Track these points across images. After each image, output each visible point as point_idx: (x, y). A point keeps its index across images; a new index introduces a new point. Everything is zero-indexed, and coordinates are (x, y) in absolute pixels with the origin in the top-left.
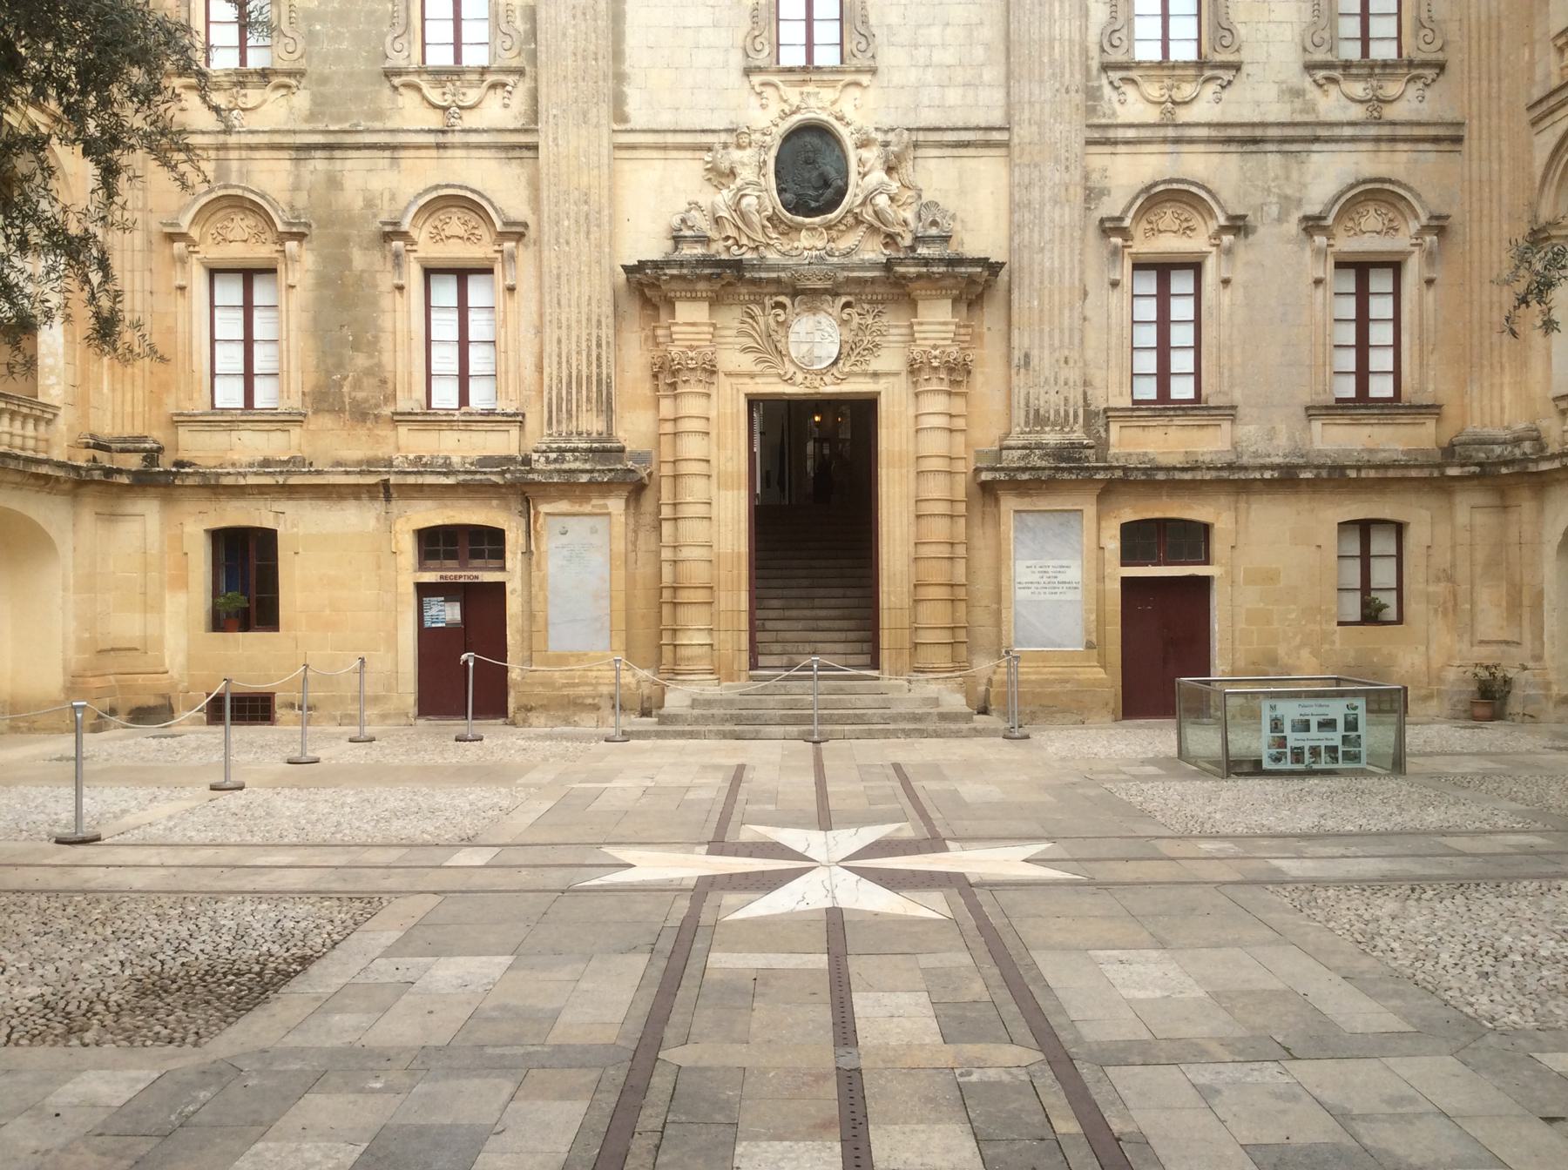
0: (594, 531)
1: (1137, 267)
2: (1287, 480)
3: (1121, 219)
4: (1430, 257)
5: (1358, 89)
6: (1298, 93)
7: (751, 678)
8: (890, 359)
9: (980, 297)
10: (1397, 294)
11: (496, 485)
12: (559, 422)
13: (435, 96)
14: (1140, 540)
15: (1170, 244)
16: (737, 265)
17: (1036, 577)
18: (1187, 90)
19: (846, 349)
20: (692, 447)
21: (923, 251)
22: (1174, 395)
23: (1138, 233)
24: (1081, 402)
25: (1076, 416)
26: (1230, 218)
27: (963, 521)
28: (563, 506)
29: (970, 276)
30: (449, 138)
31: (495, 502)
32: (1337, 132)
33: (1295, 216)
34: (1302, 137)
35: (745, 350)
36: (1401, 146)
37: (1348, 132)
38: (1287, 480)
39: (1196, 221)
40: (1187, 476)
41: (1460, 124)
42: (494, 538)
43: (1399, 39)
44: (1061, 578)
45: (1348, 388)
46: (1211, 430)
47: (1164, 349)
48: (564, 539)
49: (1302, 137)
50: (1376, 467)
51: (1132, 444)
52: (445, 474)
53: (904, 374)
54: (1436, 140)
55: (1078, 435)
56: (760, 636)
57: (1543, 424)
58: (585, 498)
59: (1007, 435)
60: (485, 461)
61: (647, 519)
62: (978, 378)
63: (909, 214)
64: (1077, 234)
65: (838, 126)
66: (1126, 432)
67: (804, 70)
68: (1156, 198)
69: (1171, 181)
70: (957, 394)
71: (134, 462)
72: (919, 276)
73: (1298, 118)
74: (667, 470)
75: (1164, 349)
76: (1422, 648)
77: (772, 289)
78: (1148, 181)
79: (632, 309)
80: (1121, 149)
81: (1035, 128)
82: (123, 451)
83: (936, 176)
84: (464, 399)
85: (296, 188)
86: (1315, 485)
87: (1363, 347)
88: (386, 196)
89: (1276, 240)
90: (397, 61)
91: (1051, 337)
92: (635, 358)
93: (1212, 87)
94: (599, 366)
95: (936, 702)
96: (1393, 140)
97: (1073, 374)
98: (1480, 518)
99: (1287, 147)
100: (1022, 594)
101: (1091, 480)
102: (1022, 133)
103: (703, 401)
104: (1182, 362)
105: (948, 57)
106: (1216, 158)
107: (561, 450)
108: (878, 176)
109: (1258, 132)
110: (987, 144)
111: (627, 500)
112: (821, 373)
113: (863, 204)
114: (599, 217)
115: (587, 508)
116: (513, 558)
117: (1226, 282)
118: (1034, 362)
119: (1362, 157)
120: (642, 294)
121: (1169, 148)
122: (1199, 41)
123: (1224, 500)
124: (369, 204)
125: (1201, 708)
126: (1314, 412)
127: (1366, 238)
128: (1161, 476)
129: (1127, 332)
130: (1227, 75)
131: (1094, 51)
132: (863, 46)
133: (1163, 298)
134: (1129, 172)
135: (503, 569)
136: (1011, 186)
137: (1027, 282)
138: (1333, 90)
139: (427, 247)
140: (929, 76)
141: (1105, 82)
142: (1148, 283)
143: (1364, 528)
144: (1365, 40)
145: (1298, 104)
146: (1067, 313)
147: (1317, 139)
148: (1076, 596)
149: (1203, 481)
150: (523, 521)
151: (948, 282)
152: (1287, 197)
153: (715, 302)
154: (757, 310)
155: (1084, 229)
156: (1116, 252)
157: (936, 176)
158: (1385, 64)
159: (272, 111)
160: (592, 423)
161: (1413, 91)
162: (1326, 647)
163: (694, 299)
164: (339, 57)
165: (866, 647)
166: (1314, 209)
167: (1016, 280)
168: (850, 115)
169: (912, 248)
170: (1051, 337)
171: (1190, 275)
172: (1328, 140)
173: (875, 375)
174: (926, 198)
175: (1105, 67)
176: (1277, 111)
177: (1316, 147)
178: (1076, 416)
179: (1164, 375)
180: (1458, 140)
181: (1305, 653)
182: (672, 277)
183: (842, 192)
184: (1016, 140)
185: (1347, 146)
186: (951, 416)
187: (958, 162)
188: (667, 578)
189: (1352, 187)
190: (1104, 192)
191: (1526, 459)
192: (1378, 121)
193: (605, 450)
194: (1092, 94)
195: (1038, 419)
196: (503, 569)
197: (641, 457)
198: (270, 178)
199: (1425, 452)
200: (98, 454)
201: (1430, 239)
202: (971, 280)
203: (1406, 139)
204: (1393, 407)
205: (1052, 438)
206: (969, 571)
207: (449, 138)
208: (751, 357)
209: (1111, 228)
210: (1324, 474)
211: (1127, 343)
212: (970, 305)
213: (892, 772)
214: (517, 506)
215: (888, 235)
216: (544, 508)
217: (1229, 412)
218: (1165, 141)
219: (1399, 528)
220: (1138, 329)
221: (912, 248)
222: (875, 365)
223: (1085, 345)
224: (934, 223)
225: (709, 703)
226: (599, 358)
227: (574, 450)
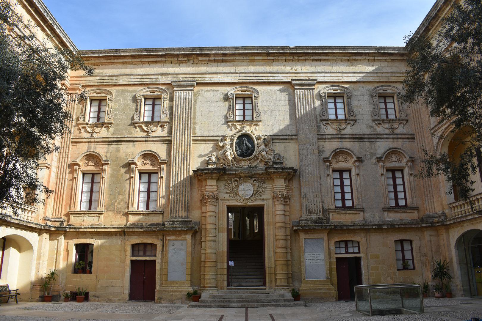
0: (182, 245)
1: (334, 171)
2: (380, 228)
3: (328, 158)
4: (411, 168)
5: (387, 126)
6: (372, 127)
7: (227, 289)
8: (267, 195)
9: (292, 178)
10: (403, 178)
11: (155, 231)
12: (173, 213)
13: (145, 128)
15: (342, 165)
16: (224, 169)
17: (311, 258)
18: (343, 126)
19: (255, 192)
20: (210, 220)
21: (275, 166)
22: (347, 205)
23: (333, 162)
24: (321, 207)
25: (320, 211)
26: (357, 158)
27: (289, 241)
28: (173, 237)
29: (289, 172)
30: (148, 139)
31: (154, 236)
32: (383, 136)
33: (374, 158)
34: (374, 137)
35: (226, 193)
36: (399, 140)
37: (386, 136)
38: (380, 228)
39: (348, 159)
40: (352, 228)
41: (414, 135)
42: (153, 246)
44: (319, 258)
45: (393, 203)
46: (358, 215)
47: (343, 193)
48: (173, 247)
49: (374, 137)
50: (403, 225)
51: (336, 218)
52: (141, 228)
53: (271, 200)
54: (408, 138)
55: (321, 216)
56: (230, 277)
57: (446, 211)
58: (180, 235)
59: (301, 216)
60: (152, 225)
61: (198, 241)
62: (292, 201)
63: (271, 157)
64: (317, 162)
65: (252, 134)
66: (334, 215)
67: (243, 121)
68: (337, 153)
69: (341, 148)
70: (286, 205)
71: (57, 224)
72: (275, 172)
73: (372, 133)
74: (203, 227)
75: (343, 193)
76: (421, 276)
77: (234, 176)
78: (335, 149)
79: (195, 182)
80: (327, 140)
81: (304, 135)
82: (54, 221)
83: (278, 147)
84: (148, 208)
85: (107, 152)
86: (387, 230)
87: (396, 192)
88: (131, 153)
89: (370, 164)
90: (136, 120)
91: (312, 189)
92: (196, 195)
93: (349, 125)
94: (185, 198)
95: (283, 296)
96: (397, 138)
97: (319, 199)
98: (432, 238)
99: (370, 140)
100: (307, 263)
101: (325, 229)
102: (301, 136)
103: (214, 207)
105: (281, 118)
106: (352, 143)
107: (173, 221)
108: (263, 147)
109: (362, 137)
110: (292, 139)
111: (192, 236)
112: (248, 199)
113: (259, 154)
114: (186, 158)
115: (180, 238)
116: (159, 254)
117: (358, 175)
118: (308, 196)
119: (390, 143)
120: (198, 178)
121: (340, 140)
122: (345, 114)
123: (362, 234)
124: (126, 156)
125: (362, 297)
127: (393, 163)
128: (345, 228)
129: (332, 188)
130: (353, 123)
131: (318, 117)
132: (258, 115)
133: (342, 179)
134: (330, 146)
135: (155, 256)
136: (299, 150)
137: (304, 174)
138: (381, 126)
139: (140, 166)
140: (276, 123)
141: (321, 124)
142: (337, 175)
143: (402, 242)
144: (387, 114)
145: (372, 130)
146: (316, 183)
147: (378, 138)
149: (357, 229)
150: (162, 242)
151: (283, 174)
152: (372, 153)
153: (218, 180)
154: (230, 182)
155: (319, 161)
156: (328, 167)
157: (278, 147)
158: (393, 120)
159: (102, 133)
160: (183, 214)
161: (401, 127)
162: (395, 277)
163: (212, 179)
164: (122, 119)
165: (262, 280)
166: (380, 156)
167: (301, 174)
168: (254, 131)
169: (273, 166)
170: (312, 189)
172: (380, 138)
173: (263, 200)
174: (276, 152)
175: (322, 120)
177: (378, 140)
178: (320, 211)
180: (414, 138)
181: (389, 279)
182: (206, 173)
183: (253, 151)
184: (299, 138)
185: (385, 140)
186: (285, 211)
187: (284, 144)
188: (203, 258)
189: (388, 150)
191: (443, 221)
192: (393, 134)
193: (186, 221)
194: (318, 127)
195: (310, 212)
196: (155, 256)
197: (195, 223)
198: (101, 150)
199: (416, 220)
200: (48, 222)
201: (410, 163)
202: (289, 174)
203: (400, 138)
204: (406, 208)
205: (314, 217)
206: (292, 256)
207: (148, 139)
208: (228, 195)
209: (326, 160)
210: (389, 226)
211: (333, 191)
212: (289, 181)
213: (269, 317)
214: (160, 237)
215: (266, 162)
216: (168, 238)
217: (362, 210)
218: (338, 138)
219: (411, 242)
220: (335, 187)
221: (273, 166)
222: (264, 197)
223: (321, 192)
224: (278, 159)
225: (214, 297)
226: (185, 196)
227: (177, 221)
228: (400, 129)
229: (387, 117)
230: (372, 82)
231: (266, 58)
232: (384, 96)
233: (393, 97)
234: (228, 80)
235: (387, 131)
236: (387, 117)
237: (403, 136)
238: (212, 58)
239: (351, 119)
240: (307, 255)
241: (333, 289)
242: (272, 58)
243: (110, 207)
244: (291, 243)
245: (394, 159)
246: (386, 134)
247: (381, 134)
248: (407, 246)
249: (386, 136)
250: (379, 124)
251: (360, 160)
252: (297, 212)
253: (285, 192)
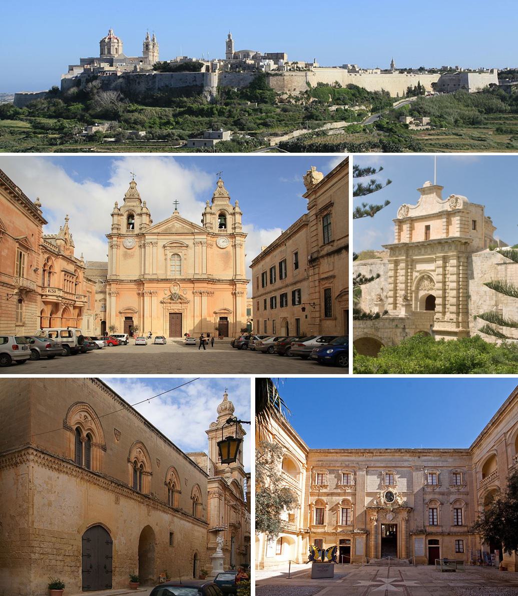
5: (457, 488)
14: (431, 542)
15: (433, 506)
47: (433, 519)
49: (450, 493)
51: (430, 529)
68: (431, 501)
75: (433, 519)
87: (457, 519)
126: (452, 526)
127: (457, 506)
142: (431, 510)
143: (459, 541)
159: (324, 490)
176: (446, 491)
179: (433, 522)
198: (325, 499)
205: (419, 529)
228: (462, 490)
234: (382, 465)
239: (440, 484)
241: (427, 560)
243: (330, 524)
245: (458, 504)
248: (461, 543)
251: (442, 504)
252: (413, 527)
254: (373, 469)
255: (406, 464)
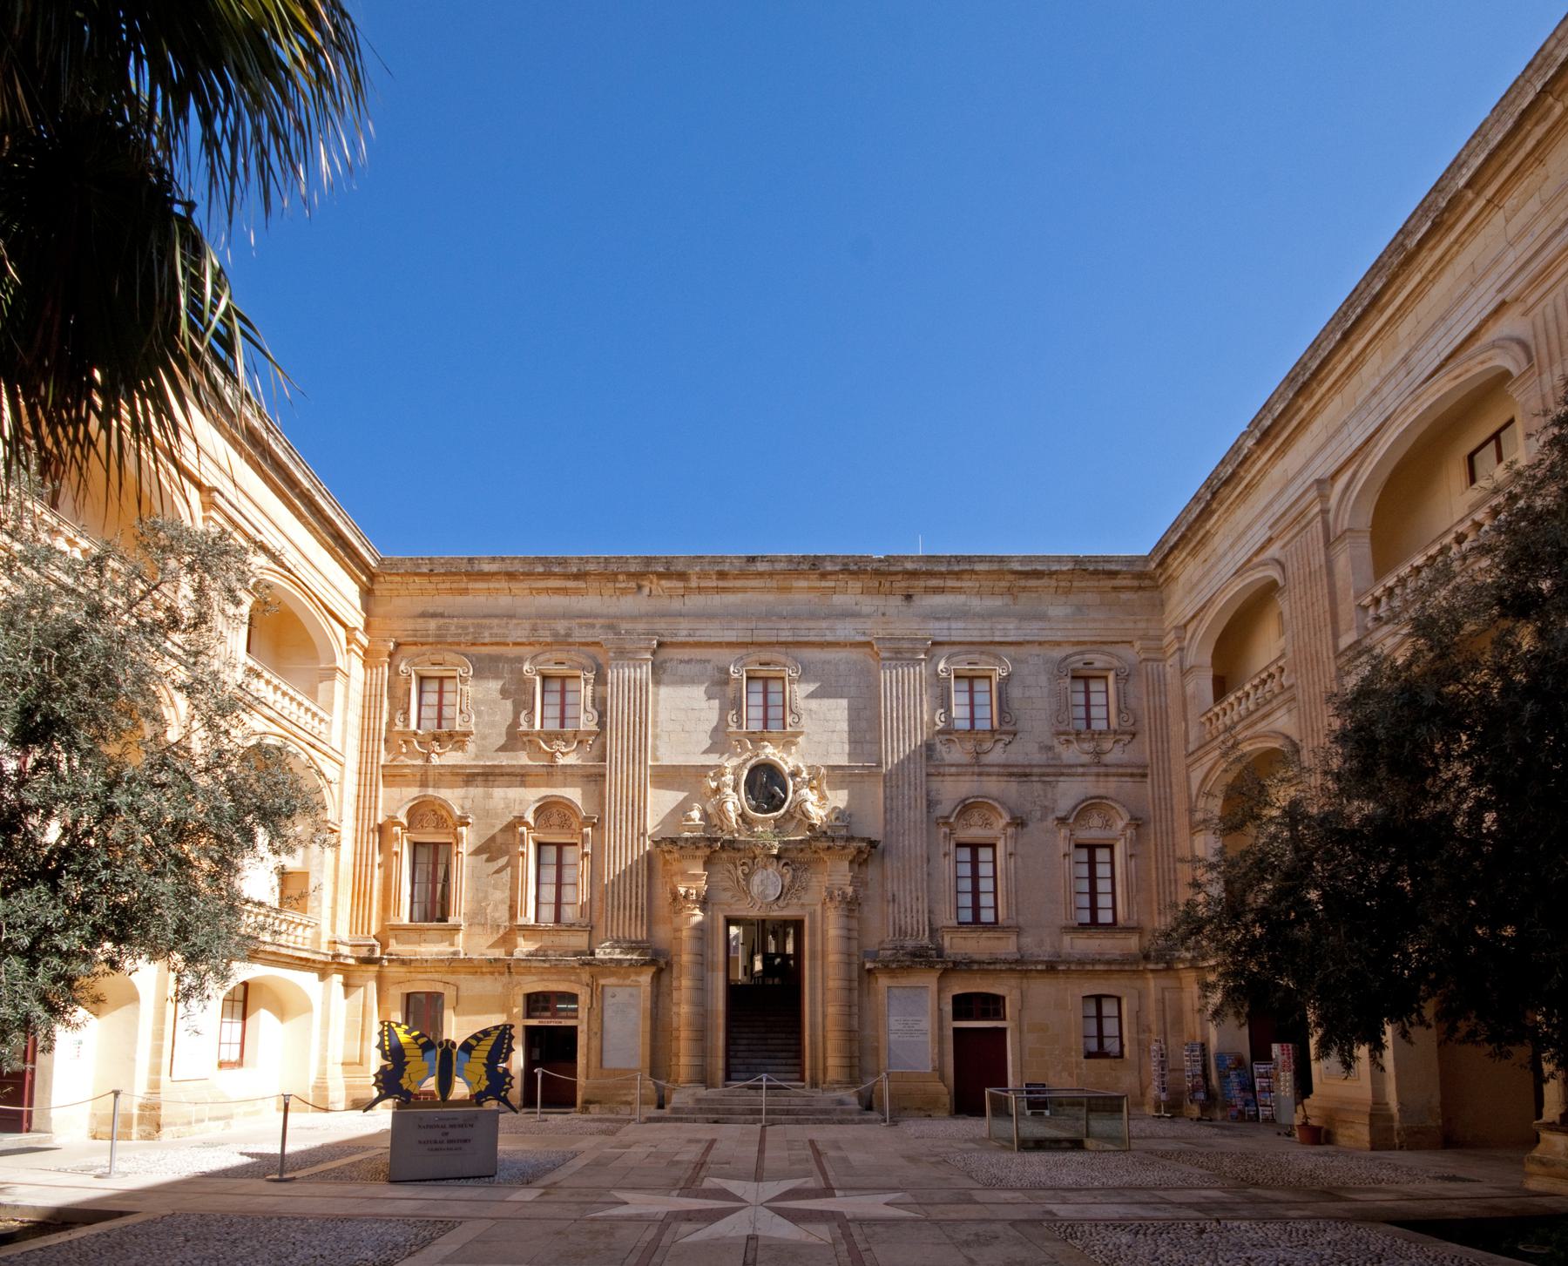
1: (959, 845)
3: (948, 817)
6: (1050, 748)
9: (866, 860)
15: (974, 833)
26: (1013, 818)
33: (1051, 818)
43: (1108, 718)
45: (1085, 917)
47: (976, 893)
51: (959, 945)
54: (1132, 775)
55: (925, 941)
68: (966, 808)
75: (976, 893)
87: (1093, 893)
93: (1001, 745)
96: (1107, 775)
97: (923, 906)
100: (893, 1037)
104: (986, 900)
106: (1003, 785)
130: (1007, 739)
134: (952, 791)
142: (965, 854)
144: (1088, 719)
145: (1050, 755)
147: (1062, 774)
148: (929, 1038)
158: (1100, 733)
161: (1118, 750)
166: (1061, 814)
171: (990, 850)
172: (1068, 775)
176: (1039, 758)
179: (976, 908)
180: (1144, 776)
190: (938, 802)
192: (1098, 764)
195: (902, 932)
205: (910, 943)
217: (1018, 930)
228: (1116, 754)
229: (1089, 726)
230: (1058, 644)
231: (817, 584)
232: (1083, 678)
233: (1106, 678)
234: (731, 636)
235: (1086, 759)
236: (1089, 726)
237: (1121, 770)
238: (694, 584)
240: (892, 1019)
242: (832, 584)
244: (860, 996)
245: (1096, 821)
246: (1083, 766)
247: (1070, 766)
249: (1080, 770)
250: (1068, 741)
251: (1019, 822)
252: (879, 932)
253: (850, 890)
254: (686, 654)
255: (845, 630)
